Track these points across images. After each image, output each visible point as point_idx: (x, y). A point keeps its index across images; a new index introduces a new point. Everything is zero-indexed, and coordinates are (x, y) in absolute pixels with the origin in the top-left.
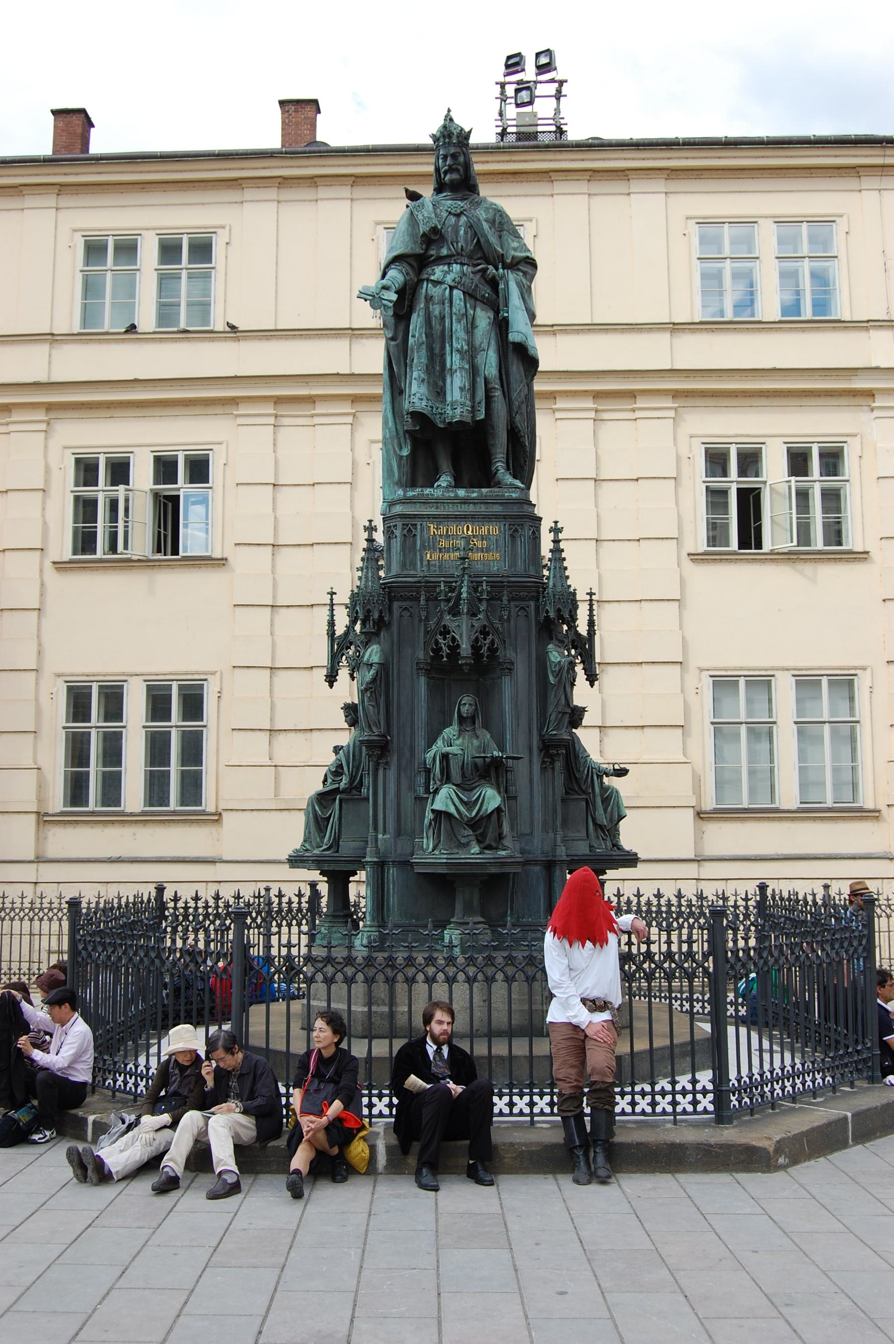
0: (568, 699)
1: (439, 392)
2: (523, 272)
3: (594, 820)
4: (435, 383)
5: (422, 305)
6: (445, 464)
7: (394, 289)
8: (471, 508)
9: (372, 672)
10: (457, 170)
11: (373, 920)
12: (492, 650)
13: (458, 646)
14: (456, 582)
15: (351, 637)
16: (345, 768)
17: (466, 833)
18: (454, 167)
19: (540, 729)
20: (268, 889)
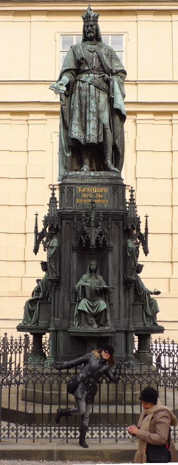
0: (135, 262)
1: (84, 130)
3: (146, 313)
4: (82, 125)
5: (77, 91)
6: (87, 161)
7: (65, 85)
9: (53, 250)
10: (93, 32)
11: (52, 355)
12: (104, 242)
13: (90, 240)
14: (89, 212)
15: (45, 234)
16: (42, 290)
17: (92, 319)
18: (91, 30)
19: (124, 275)
20: (6, 334)
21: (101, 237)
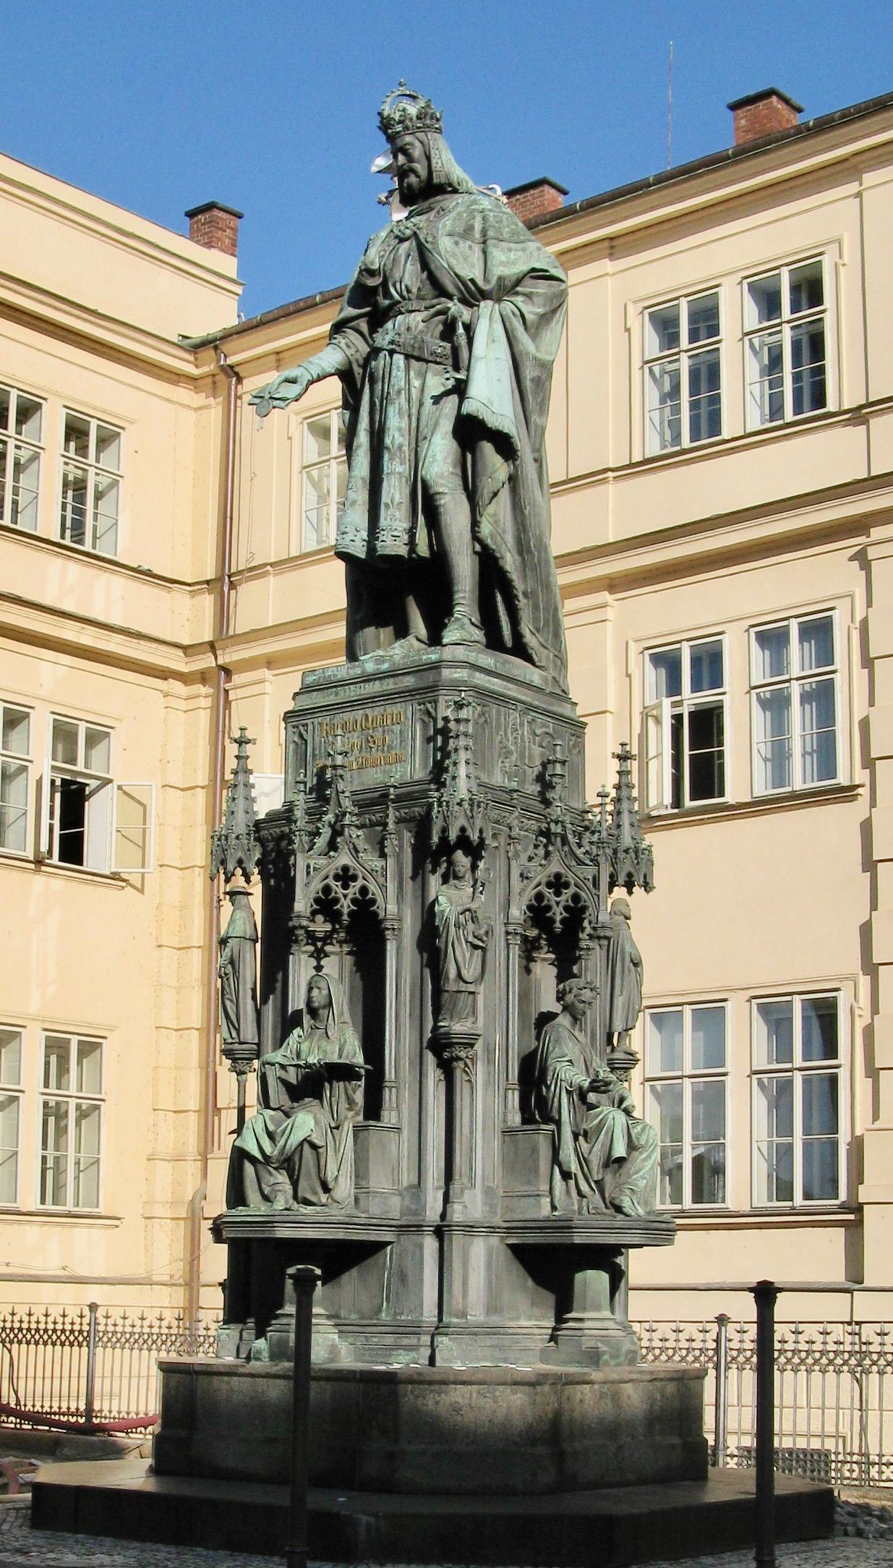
2: (524, 295)
8: (376, 687)
21: (345, 887)
